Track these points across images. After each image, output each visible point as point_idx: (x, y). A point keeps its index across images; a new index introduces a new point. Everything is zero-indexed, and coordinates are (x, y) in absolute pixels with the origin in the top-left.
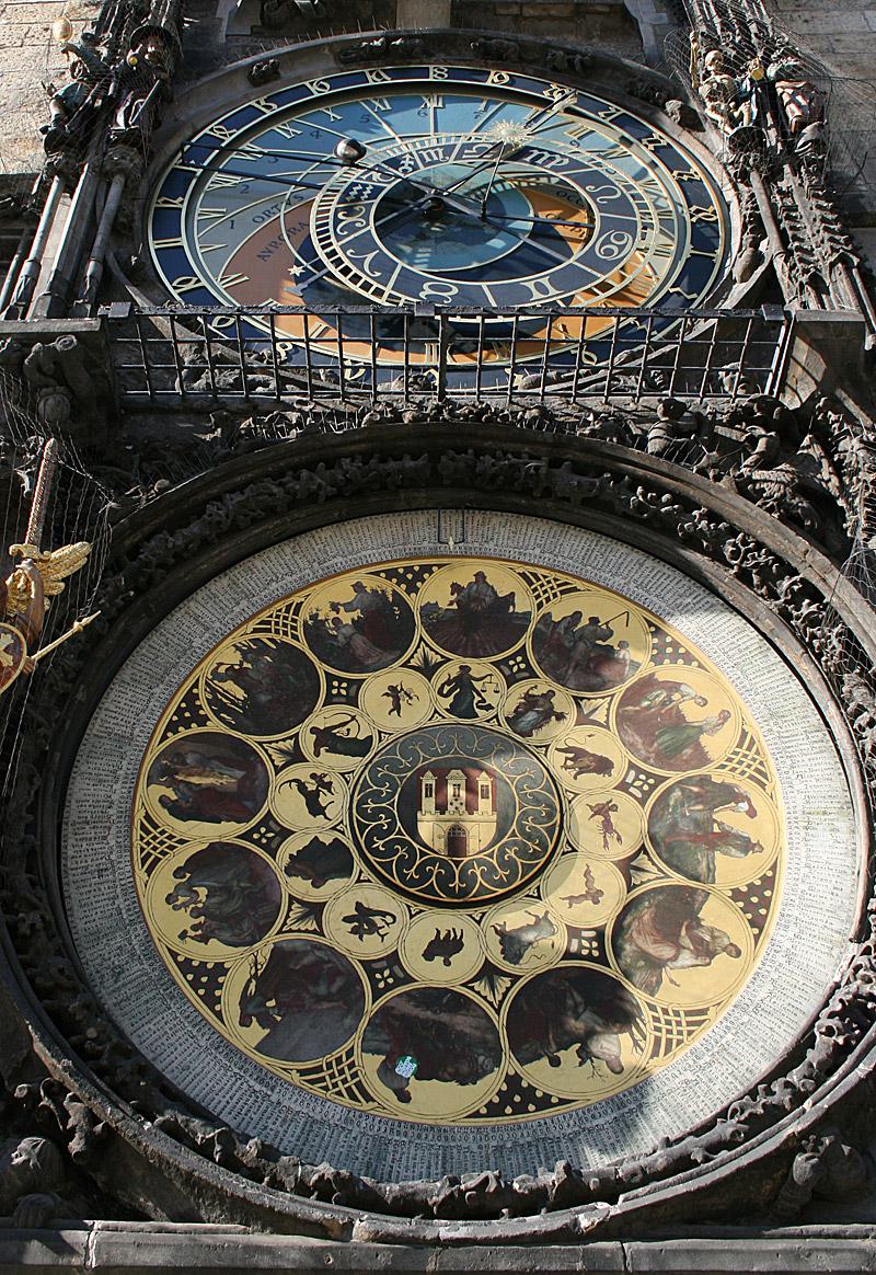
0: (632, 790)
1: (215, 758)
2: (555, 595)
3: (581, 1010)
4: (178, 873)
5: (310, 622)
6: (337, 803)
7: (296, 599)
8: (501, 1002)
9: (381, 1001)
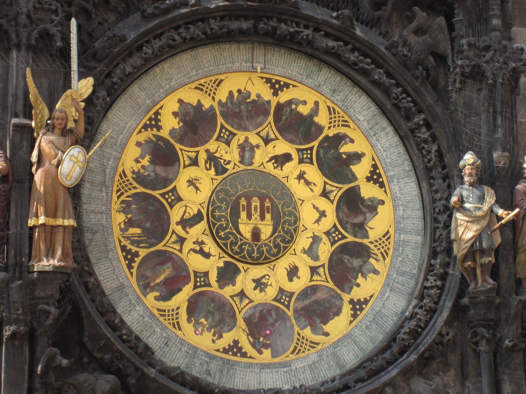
0: (305, 160)
1: (157, 264)
2: (216, 89)
3: (351, 260)
4: (189, 321)
5: (134, 176)
6: (210, 246)
7: (120, 169)
8: (326, 278)
9: (291, 308)
